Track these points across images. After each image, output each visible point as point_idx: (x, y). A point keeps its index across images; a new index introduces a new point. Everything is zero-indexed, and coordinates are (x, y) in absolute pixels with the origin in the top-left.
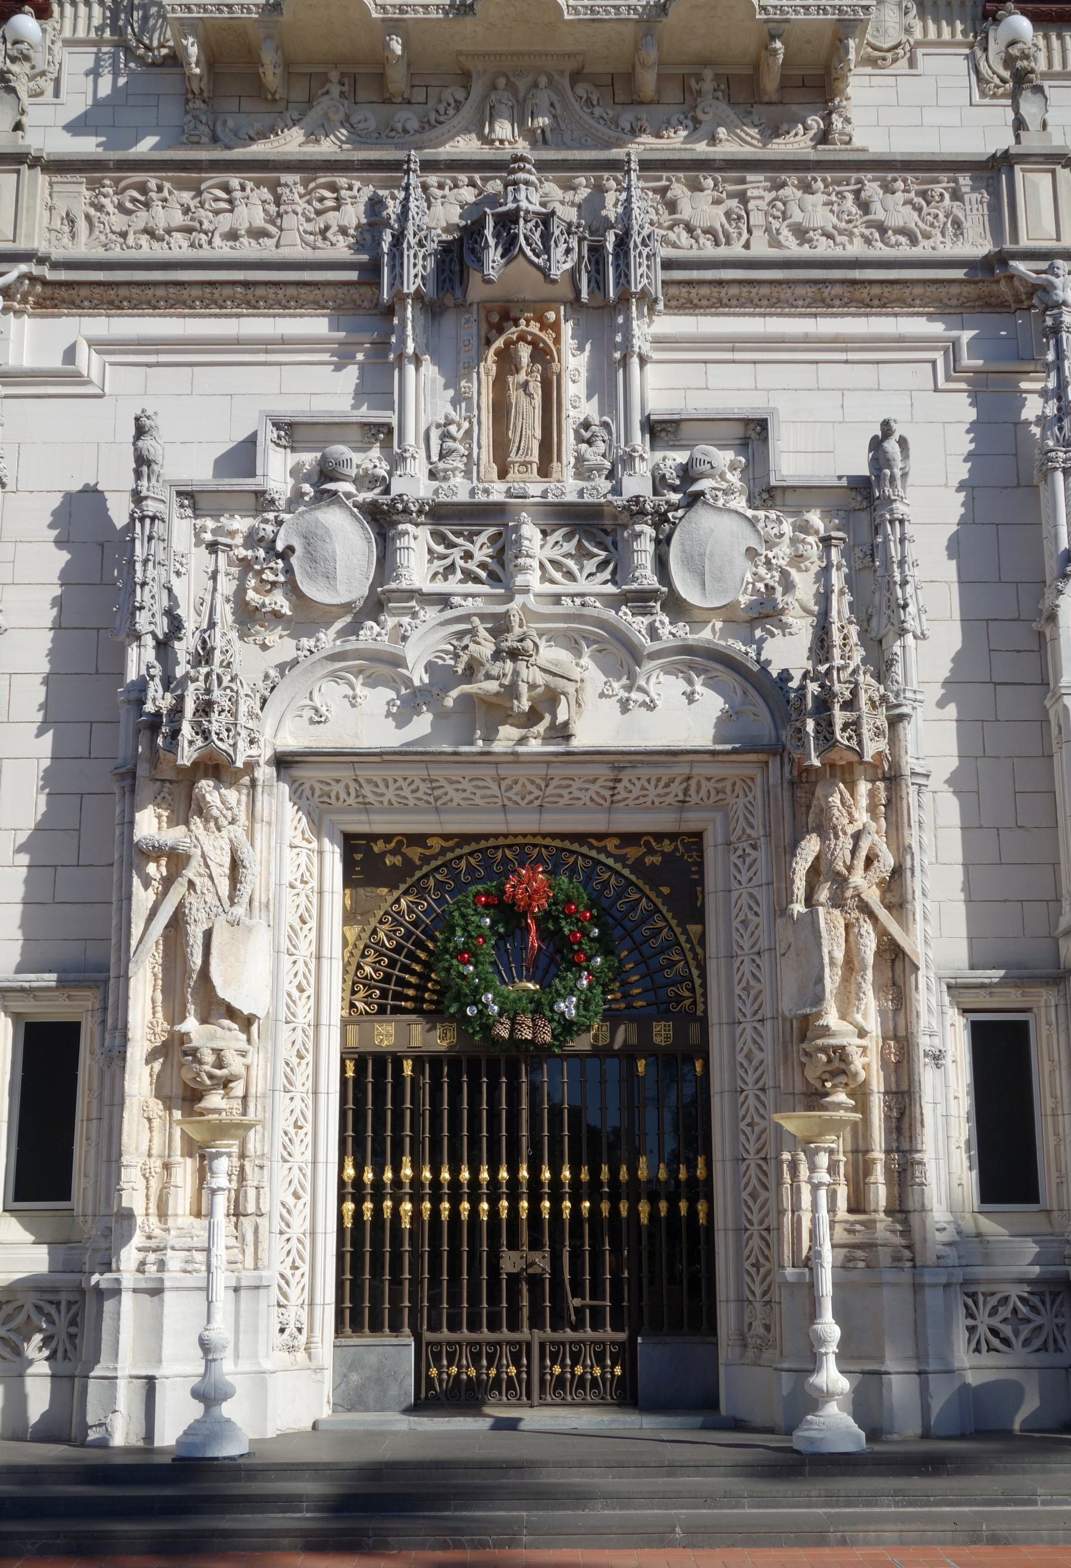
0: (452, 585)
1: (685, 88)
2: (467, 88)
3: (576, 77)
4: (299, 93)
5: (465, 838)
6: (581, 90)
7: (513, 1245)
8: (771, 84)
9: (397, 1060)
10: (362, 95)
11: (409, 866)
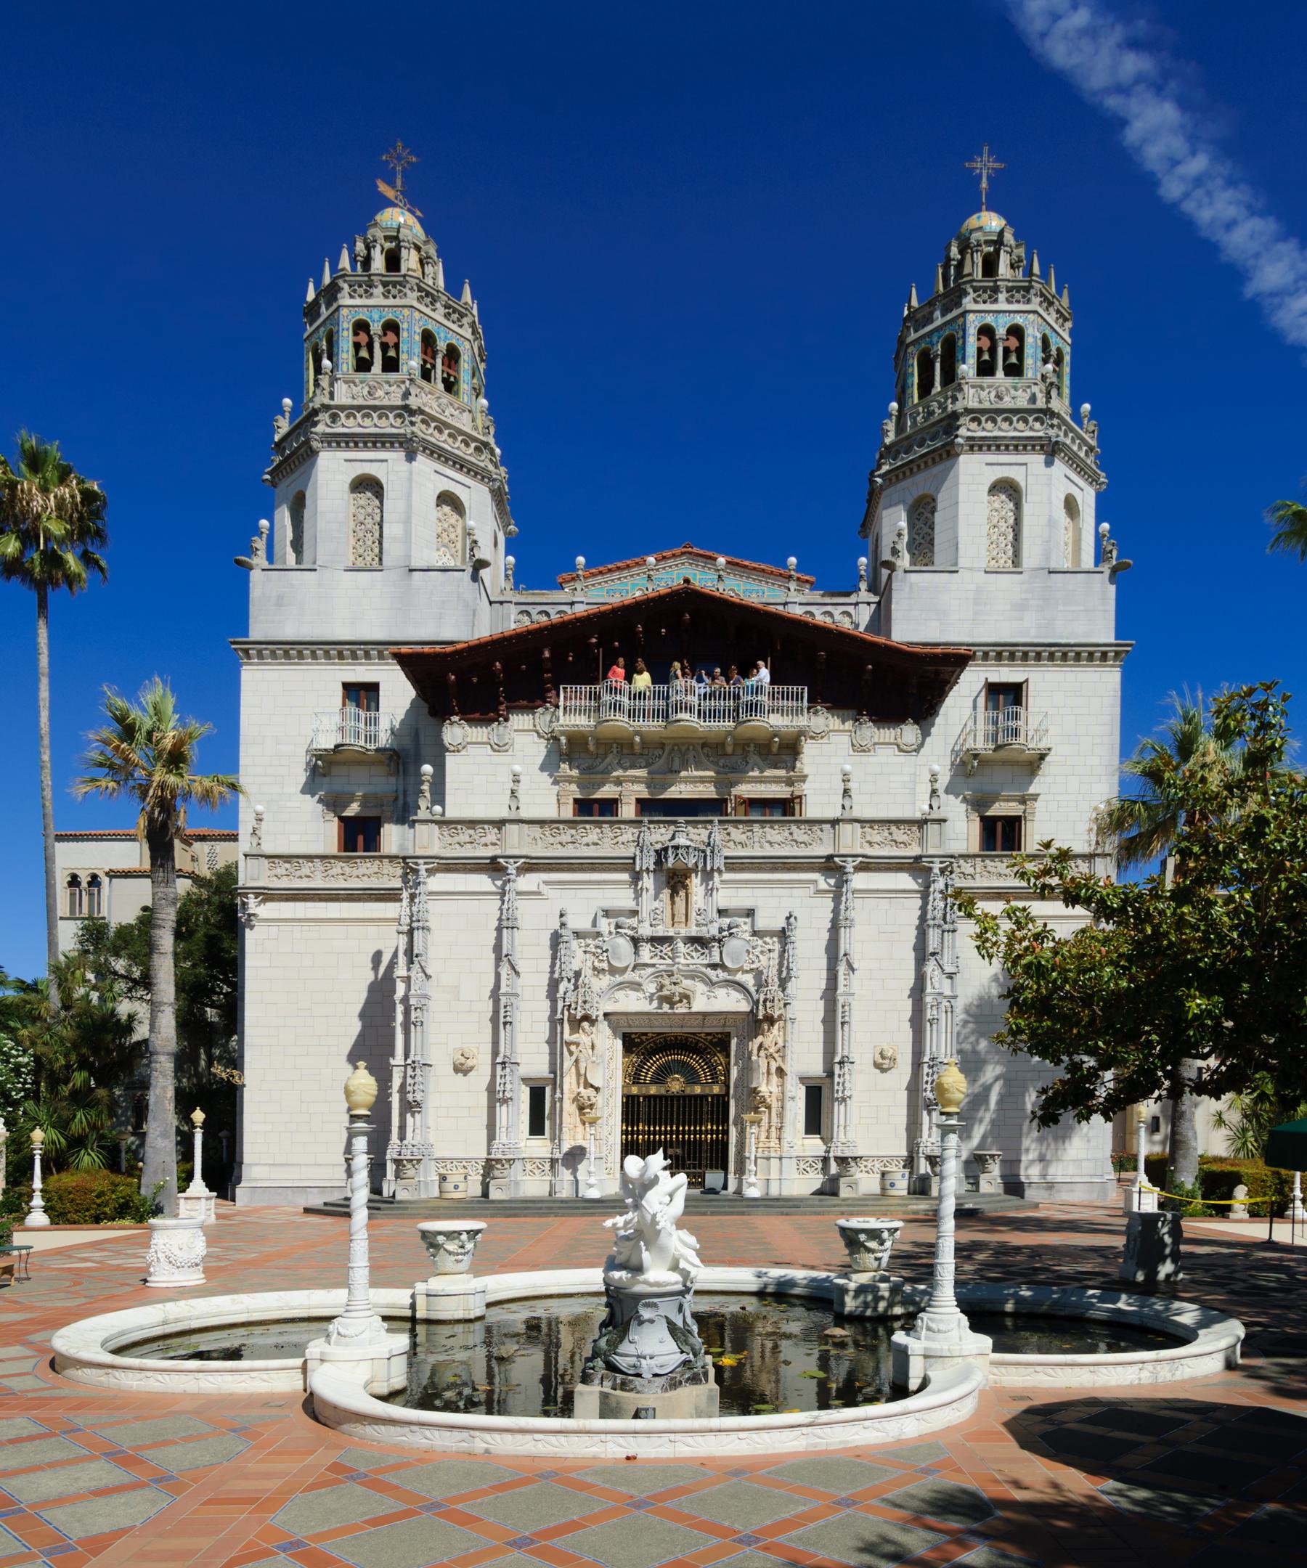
0: (654, 961)
1: (744, 749)
2: (663, 749)
3: (704, 745)
4: (601, 751)
5: (659, 1034)
6: (705, 750)
7: (671, 1147)
8: (775, 748)
9: (638, 1097)
10: (625, 751)
11: (642, 1042)
